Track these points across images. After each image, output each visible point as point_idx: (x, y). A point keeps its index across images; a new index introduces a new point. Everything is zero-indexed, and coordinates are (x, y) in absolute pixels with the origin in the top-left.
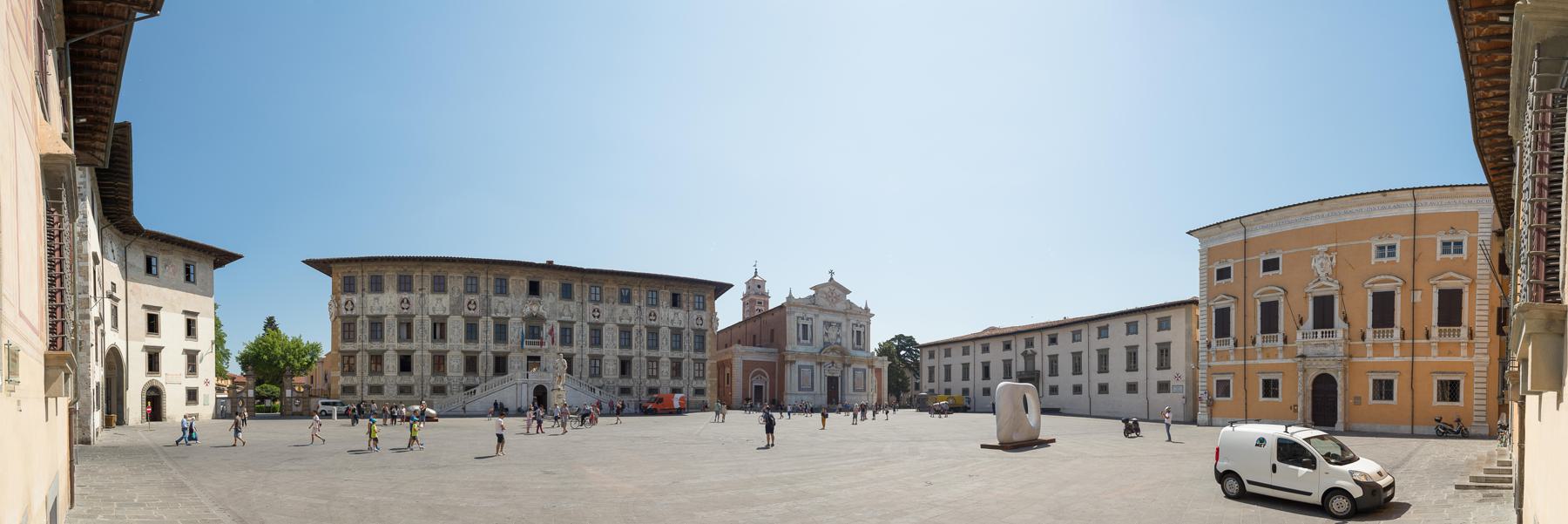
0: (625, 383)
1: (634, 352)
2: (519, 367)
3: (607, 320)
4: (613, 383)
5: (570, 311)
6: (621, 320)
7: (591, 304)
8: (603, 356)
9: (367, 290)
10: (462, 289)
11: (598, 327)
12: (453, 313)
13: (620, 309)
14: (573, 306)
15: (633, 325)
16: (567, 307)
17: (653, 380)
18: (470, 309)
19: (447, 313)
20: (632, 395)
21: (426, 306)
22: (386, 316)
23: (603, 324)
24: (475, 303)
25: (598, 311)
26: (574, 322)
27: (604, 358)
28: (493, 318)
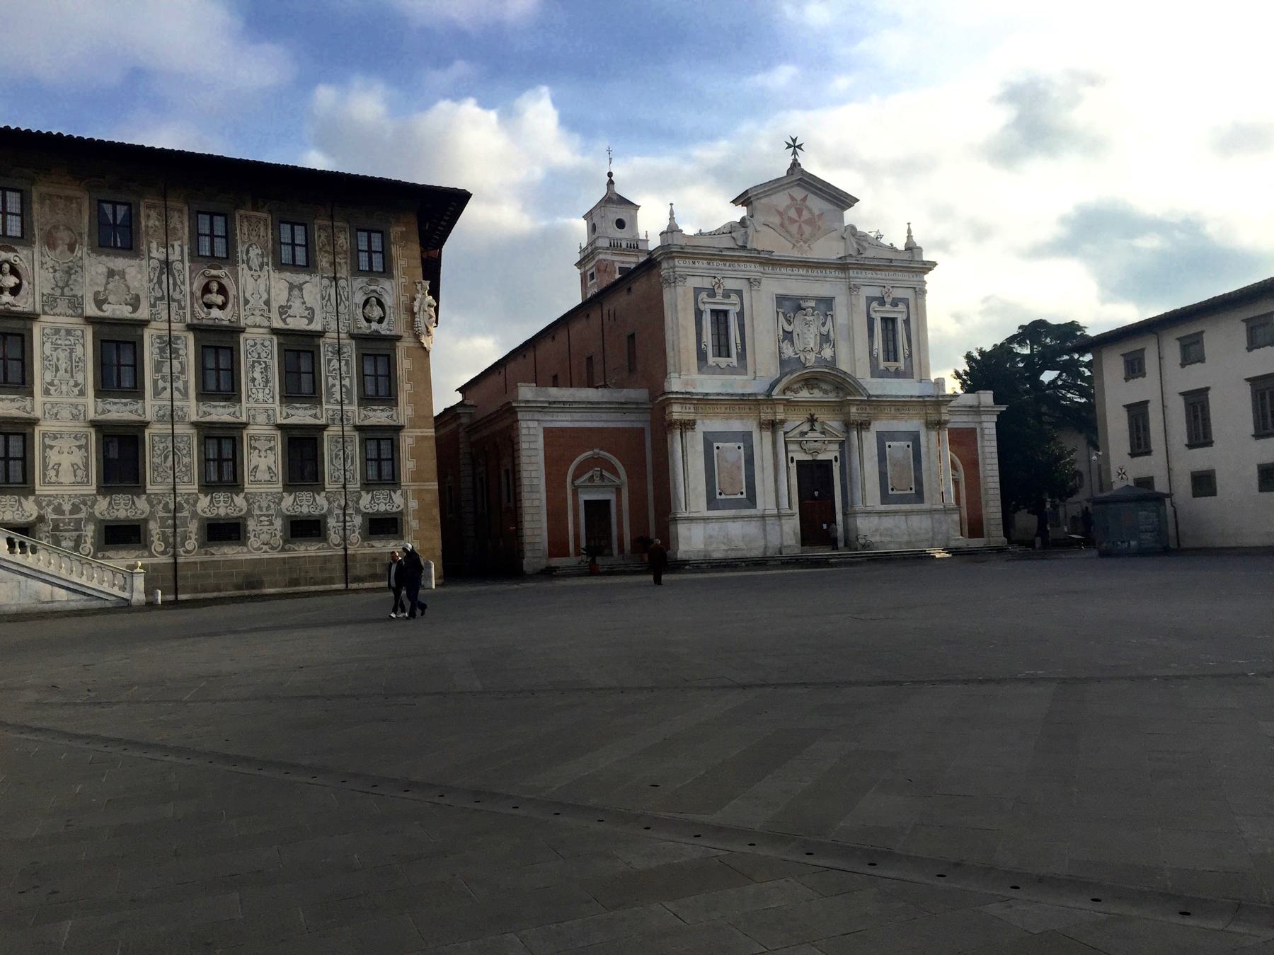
1: (150, 408)
3: (50, 302)
4: (75, 509)
6: (99, 303)
8: (33, 422)
15: (144, 324)
23: (32, 317)
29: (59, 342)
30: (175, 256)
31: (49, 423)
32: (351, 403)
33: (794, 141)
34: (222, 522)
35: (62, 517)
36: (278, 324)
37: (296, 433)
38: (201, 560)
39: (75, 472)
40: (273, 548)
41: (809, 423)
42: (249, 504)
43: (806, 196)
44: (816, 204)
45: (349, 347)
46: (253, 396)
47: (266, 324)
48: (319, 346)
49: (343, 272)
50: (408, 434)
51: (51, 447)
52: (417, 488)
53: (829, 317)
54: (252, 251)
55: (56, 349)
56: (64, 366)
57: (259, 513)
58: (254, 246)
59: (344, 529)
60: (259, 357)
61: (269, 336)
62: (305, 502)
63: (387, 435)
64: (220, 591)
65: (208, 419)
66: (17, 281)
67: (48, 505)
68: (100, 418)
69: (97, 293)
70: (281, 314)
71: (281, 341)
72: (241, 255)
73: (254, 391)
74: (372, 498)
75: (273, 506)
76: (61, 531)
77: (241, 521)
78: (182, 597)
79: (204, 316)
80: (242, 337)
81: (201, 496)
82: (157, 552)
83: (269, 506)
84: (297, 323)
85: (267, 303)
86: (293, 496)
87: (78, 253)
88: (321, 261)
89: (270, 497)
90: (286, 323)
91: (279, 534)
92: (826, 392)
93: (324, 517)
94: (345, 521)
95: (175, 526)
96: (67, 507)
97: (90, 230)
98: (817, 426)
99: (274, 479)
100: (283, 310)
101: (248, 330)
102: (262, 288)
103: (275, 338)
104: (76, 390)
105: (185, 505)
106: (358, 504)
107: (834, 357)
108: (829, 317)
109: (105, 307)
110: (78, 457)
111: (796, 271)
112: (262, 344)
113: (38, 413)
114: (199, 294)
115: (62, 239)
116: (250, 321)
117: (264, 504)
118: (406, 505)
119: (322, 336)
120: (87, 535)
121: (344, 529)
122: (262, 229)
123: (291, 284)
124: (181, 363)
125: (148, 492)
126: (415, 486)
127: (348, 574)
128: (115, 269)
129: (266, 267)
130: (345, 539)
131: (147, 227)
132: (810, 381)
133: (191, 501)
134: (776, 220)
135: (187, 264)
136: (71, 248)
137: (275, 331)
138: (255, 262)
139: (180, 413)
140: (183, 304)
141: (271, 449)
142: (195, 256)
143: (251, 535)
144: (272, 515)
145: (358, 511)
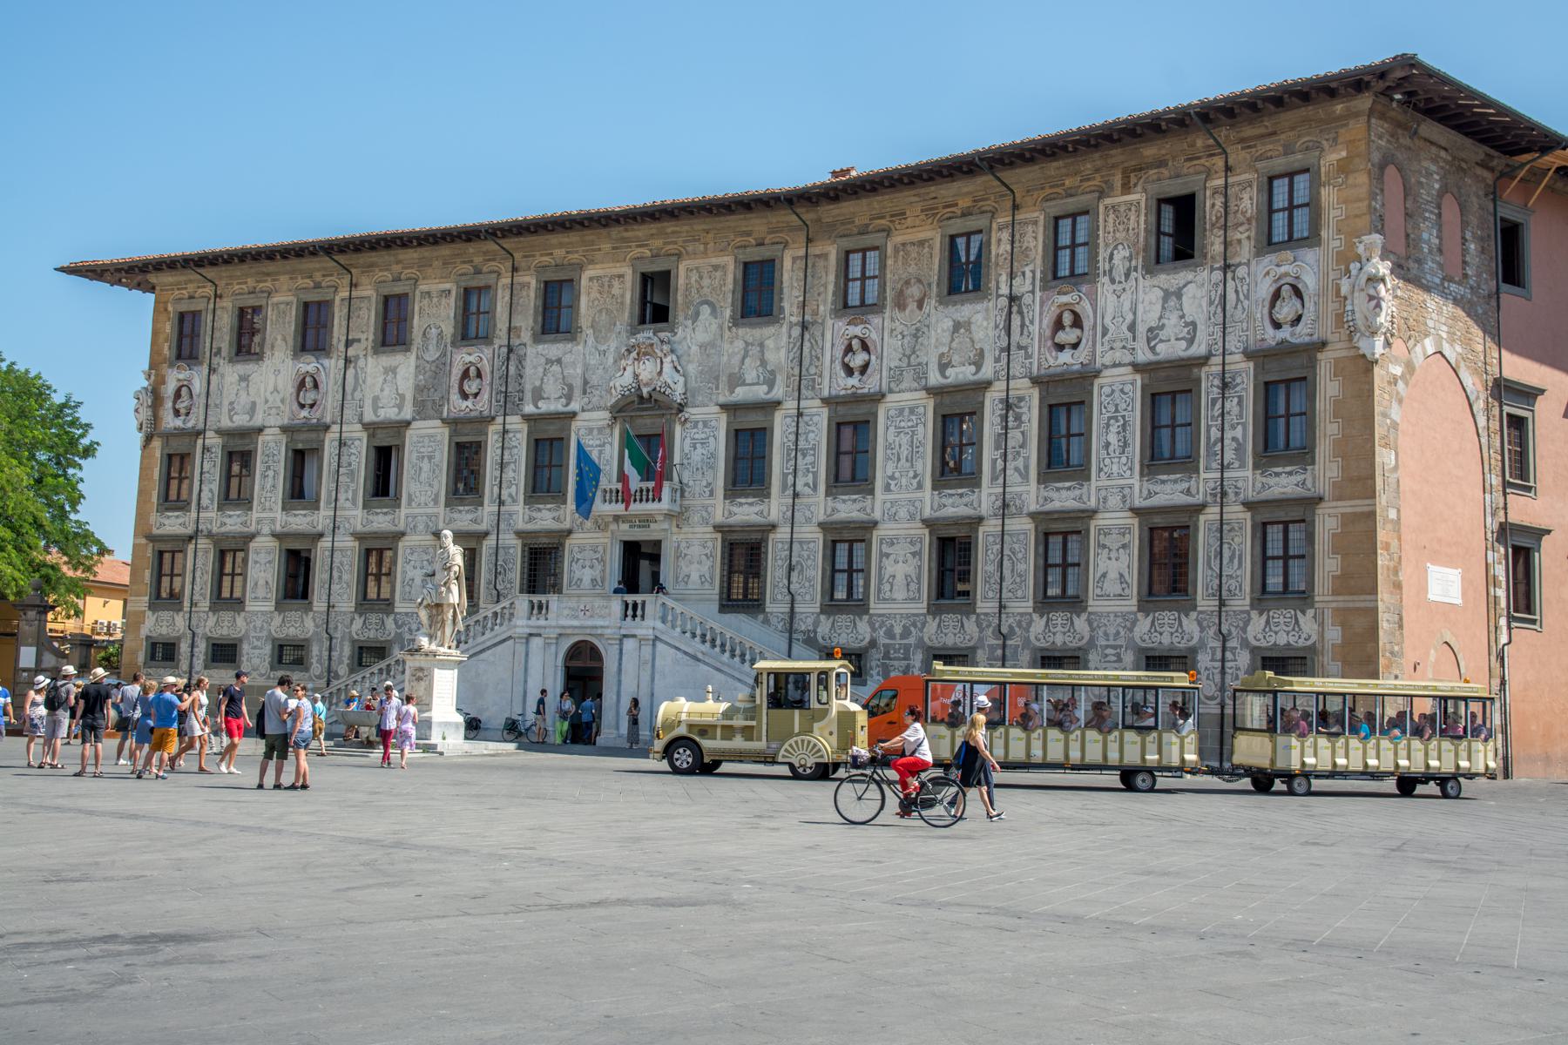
2: (594, 581)
3: (897, 375)
4: (906, 633)
5: (763, 363)
6: (943, 368)
7: (841, 324)
8: (875, 524)
9: (224, 353)
10: (448, 329)
11: (859, 412)
12: (422, 410)
13: (941, 319)
14: (776, 342)
15: (986, 385)
16: (755, 350)
17: (1059, 618)
18: (465, 396)
19: (407, 413)
21: (358, 395)
22: (260, 430)
23: (878, 397)
24: (479, 375)
25: (865, 347)
27: (876, 535)
28: (528, 418)
29: (902, 424)
30: (1022, 286)
32: (1243, 466)
34: (1057, 654)
36: (1143, 356)
37: (1158, 521)
42: (1092, 630)
47: (1128, 359)
48: (1199, 380)
49: (1245, 251)
50: (1331, 511)
51: (888, 556)
52: (1341, 605)
56: (906, 452)
58: (1120, 247)
59: (1223, 672)
60: (1117, 411)
61: (1130, 377)
62: (1166, 628)
63: (1295, 514)
65: (1049, 507)
66: (867, 357)
67: (881, 627)
68: (938, 514)
71: (1147, 381)
72: (1103, 265)
73: (1107, 461)
74: (1268, 622)
75: (1122, 633)
77: (1080, 654)
79: (1051, 362)
80: (1097, 382)
81: (1035, 617)
83: (1118, 633)
85: (1132, 327)
86: (1150, 618)
87: (926, 308)
88: (1212, 245)
89: (1119, 620)
94: (1223, 660)
96: (898, 630)
99: (1127, 592)
103: (1138, 378)
104: (915, 482)
105: (1017, 629)
106: (1245, 632)
109: (949, 371)
113: (877, 515)
114: (1048, 333)
115: (912, 296)
116: (1107, 360)
117: (1112, 631)
118: (1322, 635)
121: (1223, 672)
122: (1133, 218)
124: (1023, 433)
125: (978, 611)
126: (1343, 601)
128: (961, 320)
129: (1134, 274)
133: (1024, 624)
135: (1038, 294)
136: (920, 306)
137: (1137, 368)
138: (1119, 273)
139: (1018, 502)
140: (1030, 350)
141: (1124, 546)
142: (1053, 277)
144: (1121, 646)
145: (1245, 643)
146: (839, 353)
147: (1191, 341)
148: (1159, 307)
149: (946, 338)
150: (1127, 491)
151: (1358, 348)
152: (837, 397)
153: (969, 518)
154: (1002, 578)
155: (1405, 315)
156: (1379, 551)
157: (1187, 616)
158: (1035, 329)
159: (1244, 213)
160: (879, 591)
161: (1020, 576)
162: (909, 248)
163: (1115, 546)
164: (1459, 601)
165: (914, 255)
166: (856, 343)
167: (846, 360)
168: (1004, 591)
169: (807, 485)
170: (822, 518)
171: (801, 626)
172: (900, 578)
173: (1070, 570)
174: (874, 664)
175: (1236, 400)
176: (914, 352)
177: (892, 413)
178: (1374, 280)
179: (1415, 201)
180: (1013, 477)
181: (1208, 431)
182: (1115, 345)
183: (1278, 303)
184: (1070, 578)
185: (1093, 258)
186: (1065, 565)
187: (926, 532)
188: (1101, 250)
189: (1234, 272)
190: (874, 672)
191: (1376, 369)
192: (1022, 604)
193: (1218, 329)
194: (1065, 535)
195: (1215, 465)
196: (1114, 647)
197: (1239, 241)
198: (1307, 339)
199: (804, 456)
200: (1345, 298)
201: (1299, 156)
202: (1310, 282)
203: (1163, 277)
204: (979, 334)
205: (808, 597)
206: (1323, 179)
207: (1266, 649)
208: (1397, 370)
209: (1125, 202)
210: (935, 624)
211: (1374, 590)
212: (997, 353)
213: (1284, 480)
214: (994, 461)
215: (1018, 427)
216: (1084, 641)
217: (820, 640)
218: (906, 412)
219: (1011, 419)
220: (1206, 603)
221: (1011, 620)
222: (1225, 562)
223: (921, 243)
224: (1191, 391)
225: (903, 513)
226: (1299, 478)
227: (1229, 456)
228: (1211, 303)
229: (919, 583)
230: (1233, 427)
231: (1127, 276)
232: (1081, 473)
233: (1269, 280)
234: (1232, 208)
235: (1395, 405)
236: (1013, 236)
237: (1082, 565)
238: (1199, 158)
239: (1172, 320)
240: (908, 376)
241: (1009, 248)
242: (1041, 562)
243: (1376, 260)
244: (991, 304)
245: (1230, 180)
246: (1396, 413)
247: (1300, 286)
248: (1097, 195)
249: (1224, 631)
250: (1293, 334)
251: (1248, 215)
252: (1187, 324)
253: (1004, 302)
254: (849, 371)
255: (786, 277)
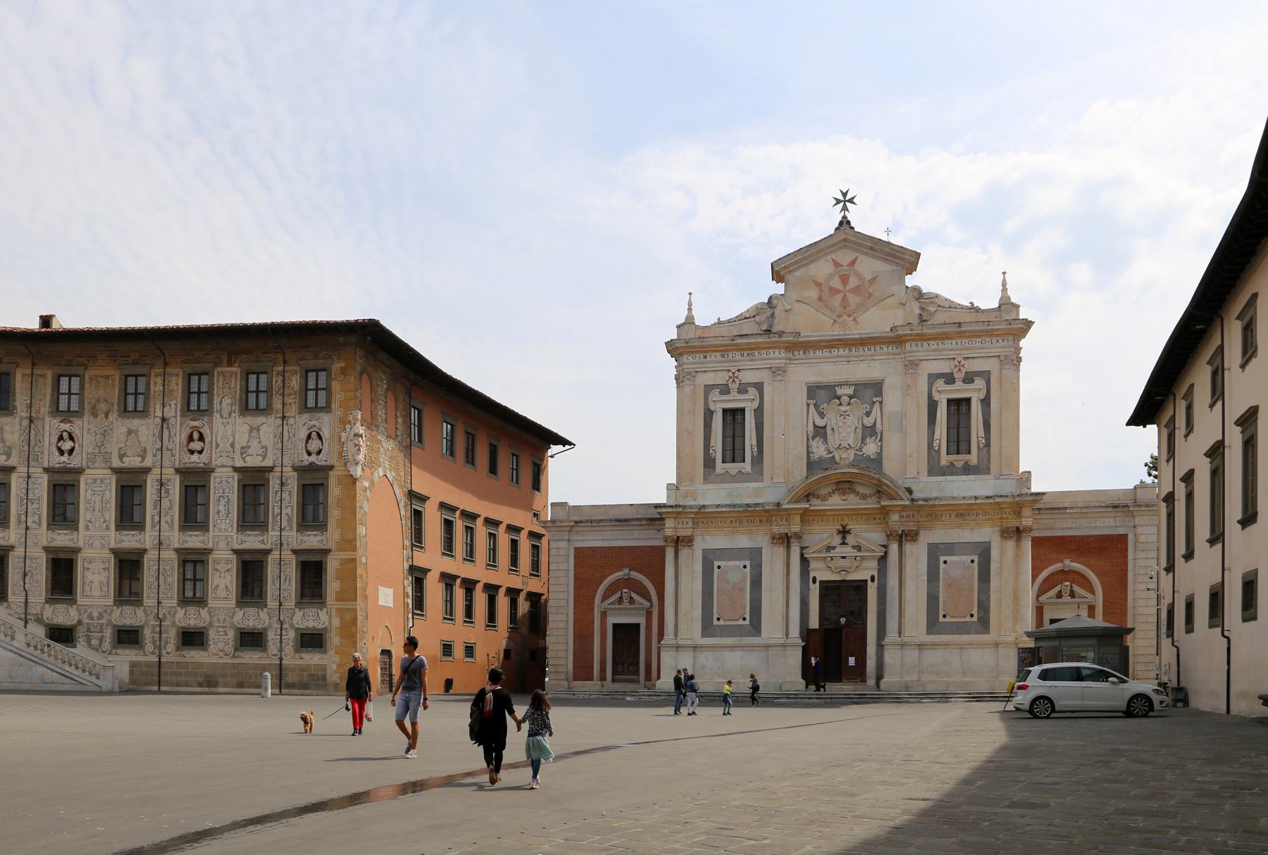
0: (128, 617)
3: (92, 458)
4: (100, 617)
6: (121, 457)
7: (55, 422)
8: (80, 549)
11: (68, 478)
13: (120, 427)
15: (147, 471)
17: (192, 610)
20: (142, 648)
23: (80, 471)
25: (71, 438)
26: (12, 469)
29: (96, 489)
30: (169, 413)
31: (89, 551)
33: (844, 194)
34: (191, 631)
35: (92, 622)
36: (239, 464)
37: (247, 557)
38: (178, 661)
39: (101, 587)
40: (226, 655)
41: (841, 536)
43: (857, 258)
44: (868, 266)
45: (292, 479)
46: (218, 526)
47: (230, 464)
48: (268, 480)
51: (88, 569)
52: (340, 607)
53: (877, 405)
54: (225, 400)
55: (94, 494)
56: (98, 506)
57: (218, 624)
59: (281, 642)
60: (224, 493)
61: (232, 474)
64: (188, 686)
65: (186, 546)
67: (84, 612)
68: (119, 546)
69: (121, 448)
70: (242, 454)
71: (240, 477)
72: (216, 406)
74: (304, 615)
75: (227, 620)
76: (91, 632)
77: (204, 630)
78: (163, 688)
79: (187, 460)
81: (178, 609)
82: (149, 652)
83: (225, 619)
84: (254, 461)
85: (232, 445)
86: (243, 611)
87: (110, 418)
88: (276, 403)
89: (226, 612)
90: (245, 462)
91: (231, 643)
92: (864, 497)
93: (265, 629)
94: (281, 635)
95: (160, 633)
96: (95, 615)
97: (118, 401)
98: (850, 539)
100: (244, 450)
101: (217, 470)
102: (229, 433)
104: (104, 525)
105: (168, 616)
107: (880, 454)
108: (877, 405)
109: (125, 459)
110: (103, 578)
111: (835, 352)
112: (227, 481)
113: (81, 544)
114: (185, 442)
115: (102, 410)
116: (219, 462)
117: (222, 618)
118: (330, 623)
119: (272, 471)
120: (106, 637)
121: (281, 642)
123: (251, 427)
124: (170, 500)
125: (145, 604)
127: (283, 681)
128: (133, 428)
129: (233, 415)
130: (281, 650)
131: (154, 392)
132: (844, 485)
133: (172, 613)
134: (813, 293)
135: (179, 419)
136: (107, 417)
137: (236, 469)
138: (225, 413)
141: (228, 570)
142: (187, 409)
143: (211, 643)
144: (227, 627)
145: (292, 626)
146: (54, 440)
147: (264, 458)
148: (247, 436)
149: (123, 438)
150: (229, 539)
151: (349, 471)
152: (54, 468)
153: (138, 549)
154: (159, 586)
155: (371, 455)
156: (358, 579)
157: (262, 610)
158: (177, 439)
159: (293, 388)
160: (83, 591)
161: (169, 585)
162: (99, 379)
163: (223, 570)
164: (392, 606)
165: (102, 384)
166: (65, 434)
167: (59, 444)
168: (160, 593)
169: (34, 522)
170: (45, 544)
171: (33, 610)
172: (96, 583)
173: (198, 583)
174: (80, 635)
175: (288, 492)
176: (103, 445)
177: (89, 481)
178: (358, 435)
179: (376, 394)
180: (164, 526)
181: (273, 508)
182: (223, 454)
183: (310, 441)
184: (198, 587)
185: (210, 401)
186: (195, 580)
187: (112, 556)
188: (215, 398)
189: (287, 420)
190: (81, 640)
191: (357, 483)
192: (171, 601)
193: (279, 452)
194: (195, 562)
195: (277, 528)
196: (223, 627)
197: (290, 404)
198: (324, 463)
199: (32, 503)
200: (344, 443)
201: (321, 362)
202: (326, 433)
203: (250, 418)
204: (143, 439)
205: (36, 593)
206: (333, 376)
207: (304, 629)
208: (367, 484)
209: (229, 372)
210: (119, 612)
211: (355, 600)
212: (155, 451)
213: (312, 538)
214: (153, 516)
215: (167, 497)
216: (206, 624)
217: (45, 619)
218: (99, 481)
219: (163, 492)
220: (272, 603)
221: (164, 611)
222: (282, 582)
223: (107, 377)
224: (264, 485)
225: (97, 543)
226: (320, 538)
227: (284, 523)
228: (275, 437)
229: (108, 586)
230: (286, 508)
231: (230, 415)
232: (204, 527)
233: (305, 428)
234: (287, 385)
235: (365, 502)
236: (164, 381)
237: (204, 580)
238: (270, 353)
239: (254, 444)
240: (99, 459)
241: (161, 388)
242: (181, 578)
243: (358, 424)
244: (150, 421)
245: (286, 368)
246: (366, 507)
247: (321, 434)
248: (213, 365)
249: (281, 619)
250: (317, 460)
251: (295, 390)
252: (262, 447)
253: (158, 421)
254: (61, 452)
255: (17, 386)
